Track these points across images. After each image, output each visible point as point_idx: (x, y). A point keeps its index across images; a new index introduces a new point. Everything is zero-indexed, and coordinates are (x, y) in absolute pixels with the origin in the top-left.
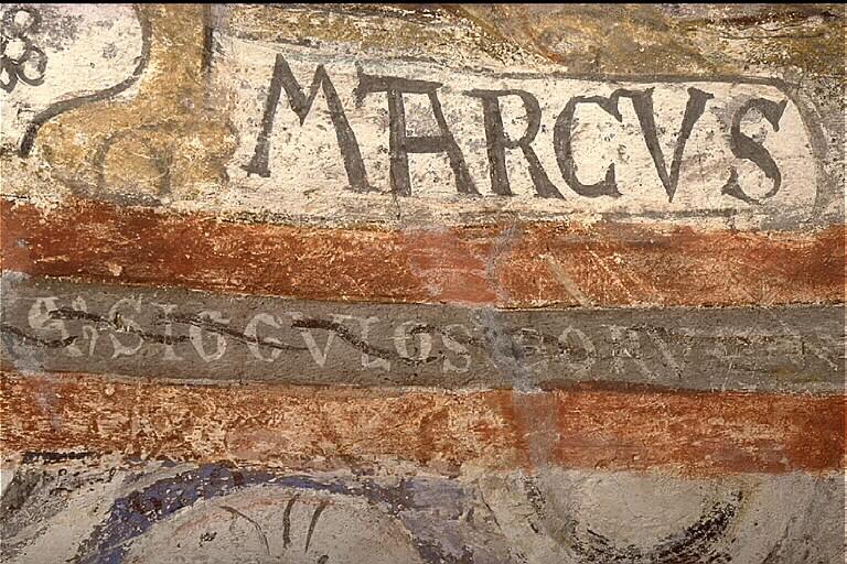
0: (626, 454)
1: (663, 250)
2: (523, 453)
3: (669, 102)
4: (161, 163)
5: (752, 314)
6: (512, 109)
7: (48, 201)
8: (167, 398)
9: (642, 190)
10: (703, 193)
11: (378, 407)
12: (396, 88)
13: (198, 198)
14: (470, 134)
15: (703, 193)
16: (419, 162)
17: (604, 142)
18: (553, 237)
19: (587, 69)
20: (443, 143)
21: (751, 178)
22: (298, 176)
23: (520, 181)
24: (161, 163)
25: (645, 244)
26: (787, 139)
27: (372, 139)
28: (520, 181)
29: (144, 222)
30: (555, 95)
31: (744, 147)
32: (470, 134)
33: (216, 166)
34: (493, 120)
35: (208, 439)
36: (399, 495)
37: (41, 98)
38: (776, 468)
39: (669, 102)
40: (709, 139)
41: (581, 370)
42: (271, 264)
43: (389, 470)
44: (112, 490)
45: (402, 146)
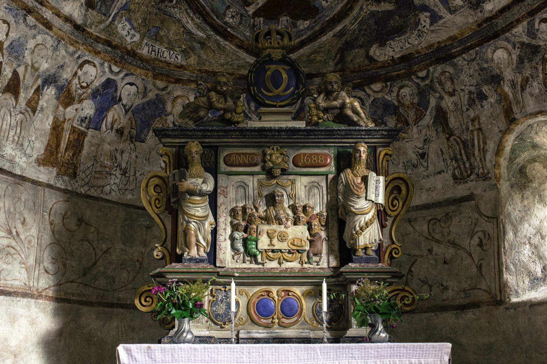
0: (162, 80)
1: (168, 64)
2: (154, 78)
3: (172, 52)
4: (137, 47)
5: (174, 70)
6: (160, 50)
7: (129, 48)
8: (131, 66)
9: (168, 58)
10: (172, 60)
11: (144, 71)
12: (153, 46)
13: (139, 51)
14: (157, 51)
15: (172, 60)
16: (153, 52)
17: (166, 54)
18: (161, 61)
19: (166, 48)
20: (155, 51)
21: (176, 60)
22: (144, 51)
23: (159, 56)
24: (137, 47)
25: (167, 63)
26: (179, 57)
27: (150, 50)
28: (159, 56)
29: (134, 52)
30: (163, 50)
31: (176, 57)
32: (157, 51)
33: (140, 49)
34: (159, 51)
35: (132, 71)
36: (143, 79)
37: (132, 41)
38: (172, 83)
39: (172, 52)
40: (174, 56)
41: (160, 72)
42: (141, 59)
43: (143, 77)
44: (125, 73)
45: (152, 51)
